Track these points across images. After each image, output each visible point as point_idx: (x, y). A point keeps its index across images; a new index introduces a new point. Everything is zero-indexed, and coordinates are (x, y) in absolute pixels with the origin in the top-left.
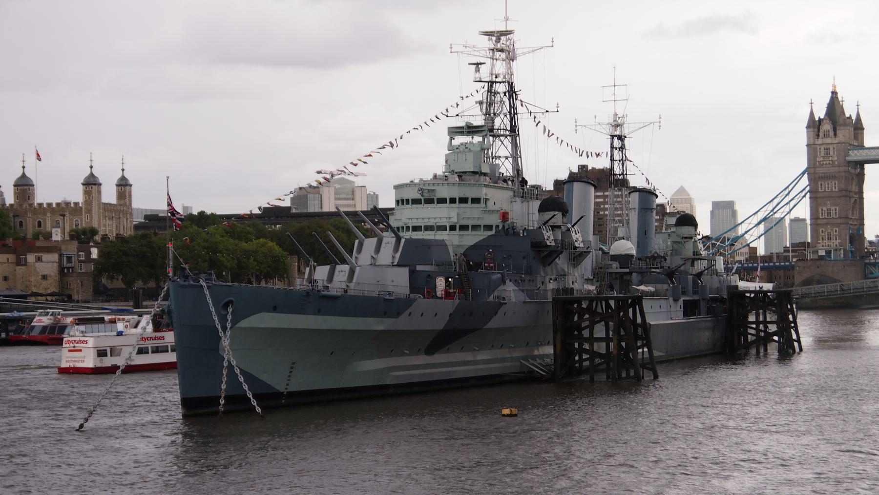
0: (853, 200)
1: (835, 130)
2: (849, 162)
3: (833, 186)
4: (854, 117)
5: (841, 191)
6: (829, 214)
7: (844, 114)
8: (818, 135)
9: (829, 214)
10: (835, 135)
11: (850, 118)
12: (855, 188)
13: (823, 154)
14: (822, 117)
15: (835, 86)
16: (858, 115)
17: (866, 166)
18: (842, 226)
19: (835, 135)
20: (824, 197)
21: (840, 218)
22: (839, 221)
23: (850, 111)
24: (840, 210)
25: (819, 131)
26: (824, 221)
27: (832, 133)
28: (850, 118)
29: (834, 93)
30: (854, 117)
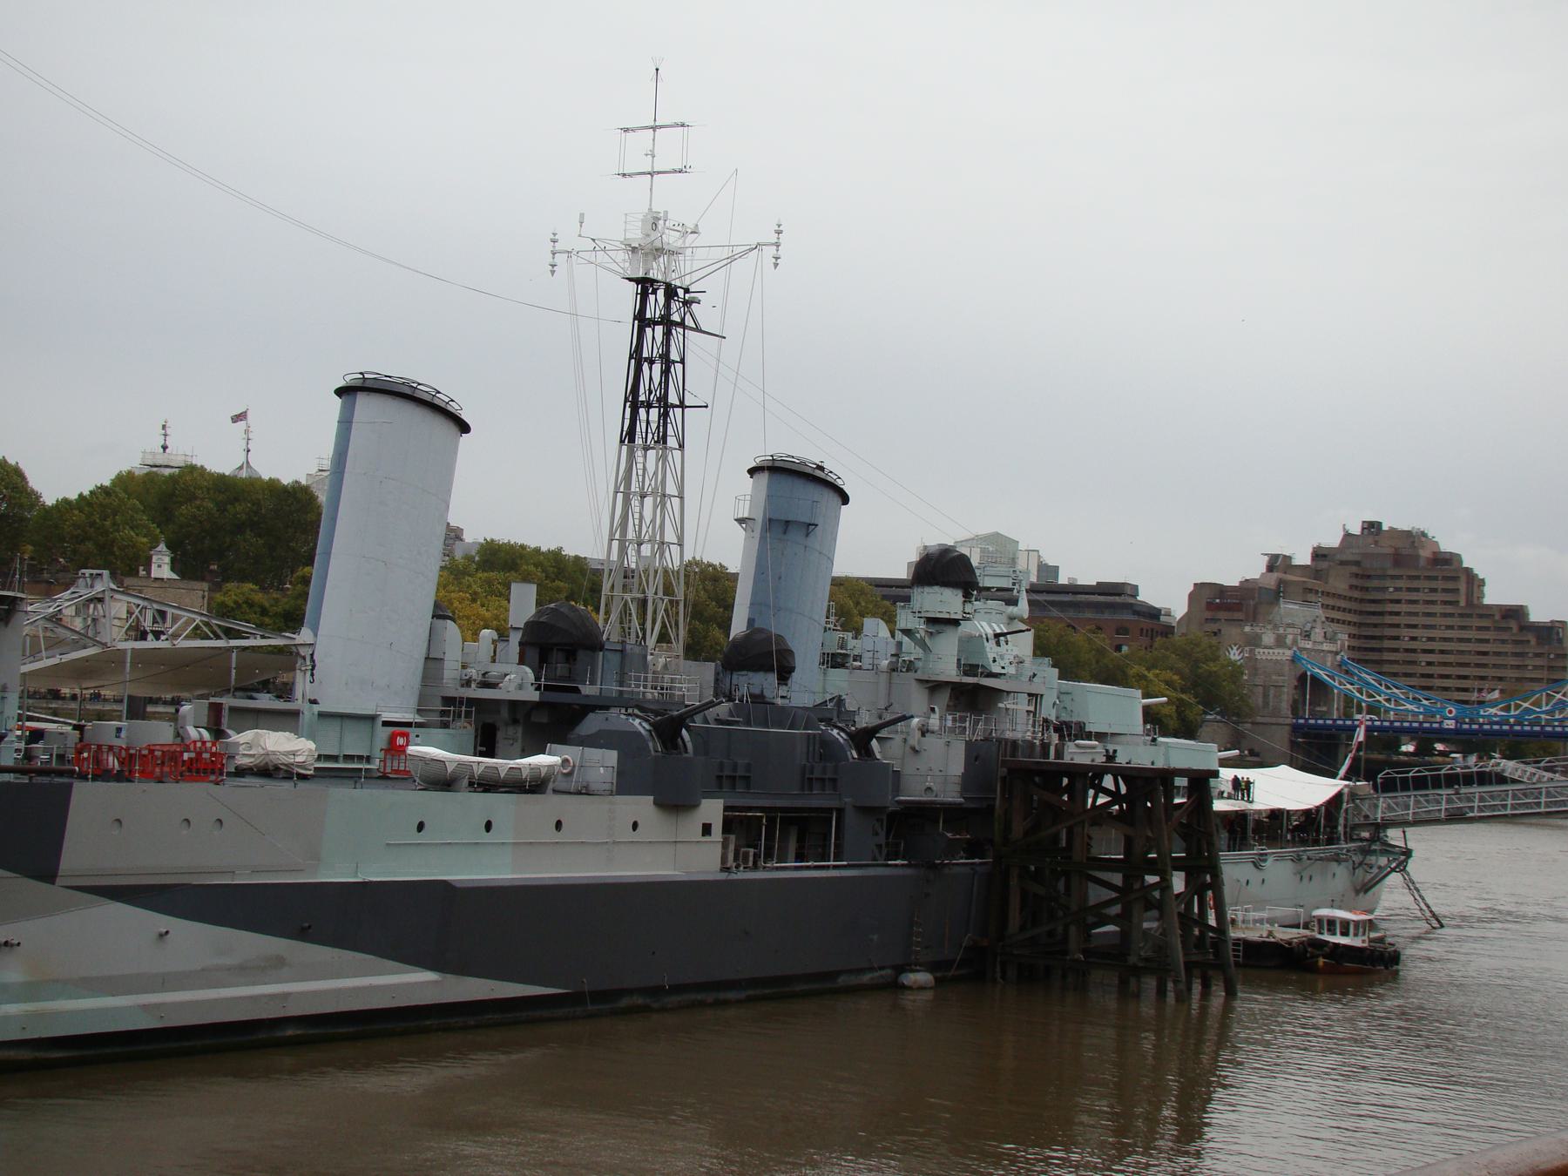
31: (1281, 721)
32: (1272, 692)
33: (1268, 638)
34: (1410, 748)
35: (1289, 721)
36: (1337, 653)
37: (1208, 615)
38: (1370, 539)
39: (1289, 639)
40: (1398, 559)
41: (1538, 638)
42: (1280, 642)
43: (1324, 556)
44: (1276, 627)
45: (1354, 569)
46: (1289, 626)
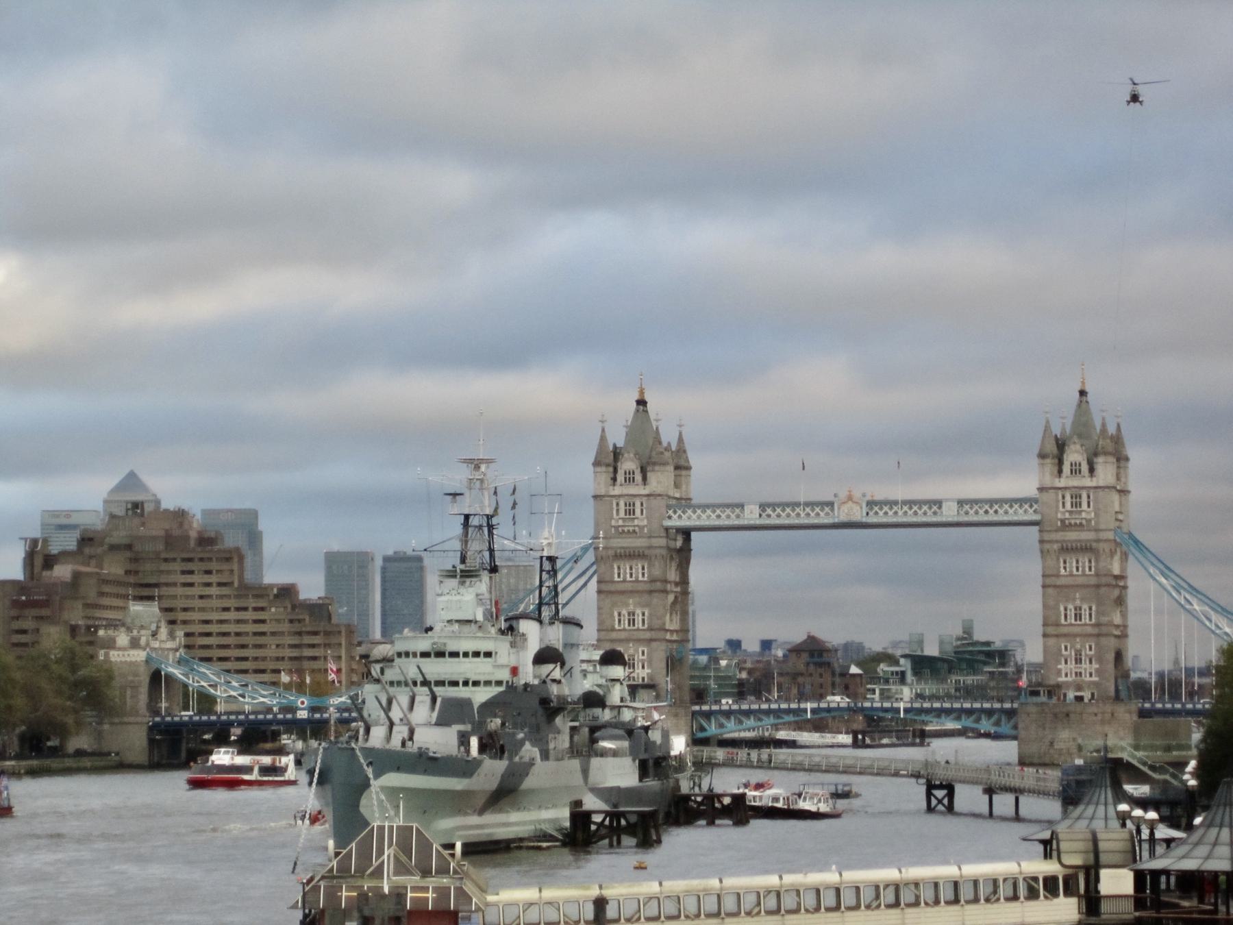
0: (671, 598)
1: (644, 471)
2: (667, 529)
3: (638, 572)
4: (674, 449)
5: (652, 581)
6: (632, 622)
7: (660, 443)
8: (614, 479)
9: (632, 622)
10: (645, 479)
11: (668, 448)
12: (673, 575)
13: (622, 514)
14: (620, 444)
15: (642, 392)
16: (681, 440)
17: (693, 534)
18: (654, 644)
19: (645, 479)
20: (622, 592)
21: (650, 629)
22: (648, 635)
23: (669, 436)
24: (650, 614)
25: (615, 471)
26: (623, 635)
27: (638, 477)
28: (668, 448)
29: (641, 403)
30: (674, 449)
31: (139, 719)
32: (129, 692)
33: (123, 639)
34: (206, 737)
35: (146, 720)
36: (177, 650)
37: (14, 613)
38: (136, 521)
39: (143, 641)
40: (170, 541)
41: (311, 616)
42: (135, 644)
43: (91, 539)
44: (129, 629)
45: (128, 554)
46: (142, 627)
